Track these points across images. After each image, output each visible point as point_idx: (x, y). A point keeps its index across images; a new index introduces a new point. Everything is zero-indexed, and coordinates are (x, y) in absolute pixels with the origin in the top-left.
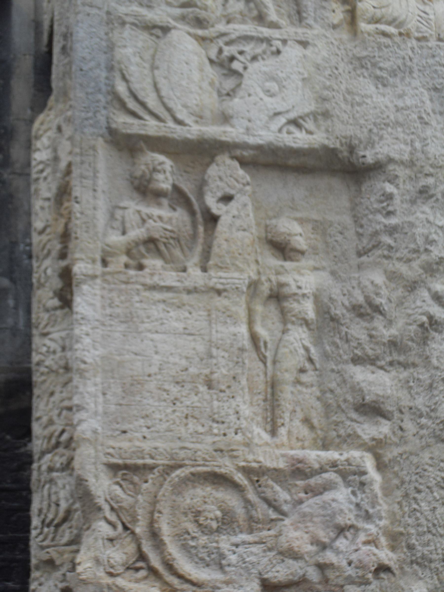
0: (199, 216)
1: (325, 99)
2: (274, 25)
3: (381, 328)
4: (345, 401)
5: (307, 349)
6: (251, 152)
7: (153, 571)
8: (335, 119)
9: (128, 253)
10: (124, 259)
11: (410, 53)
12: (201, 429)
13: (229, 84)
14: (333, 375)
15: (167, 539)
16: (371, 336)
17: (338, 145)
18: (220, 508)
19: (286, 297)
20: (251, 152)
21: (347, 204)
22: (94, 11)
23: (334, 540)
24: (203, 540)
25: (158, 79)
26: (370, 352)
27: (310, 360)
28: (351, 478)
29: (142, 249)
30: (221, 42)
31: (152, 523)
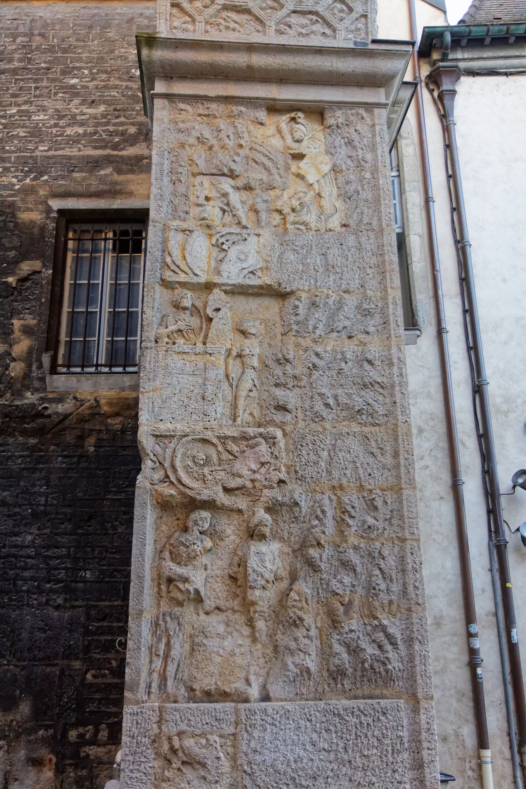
0: (204, 318)
1: (267, 261)
2: (245, 227)
3: (289, 370)
4: (270, 404)
5: (253, 380)
6: (231, 287)
7: (172, 483)
8: (272, 271)
9: (168, 337)
10: (166, 340)
11: (311, 237)
12: (198, 419)
13: (222, 255)
14: (266, 393)
15: (179, 469)
16: (284, 374)
17: (273, 283)
18: (205, 455)
19: (244, 356)
20: (231, 287)
21: (278, 311)
22: (158, 224)
23: (259, 469)
24: (196, 469)
25: (186, 255)
26: (284, 381)
27: (255, 385)
28: (269, 440)
29: (176, 335)
30: (218, 236)
31: (172, 461)
